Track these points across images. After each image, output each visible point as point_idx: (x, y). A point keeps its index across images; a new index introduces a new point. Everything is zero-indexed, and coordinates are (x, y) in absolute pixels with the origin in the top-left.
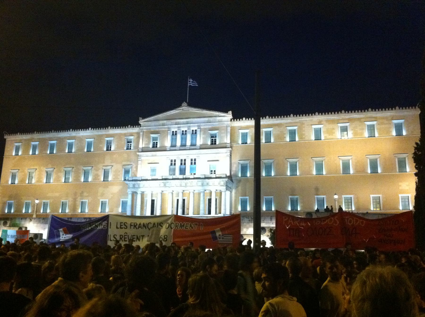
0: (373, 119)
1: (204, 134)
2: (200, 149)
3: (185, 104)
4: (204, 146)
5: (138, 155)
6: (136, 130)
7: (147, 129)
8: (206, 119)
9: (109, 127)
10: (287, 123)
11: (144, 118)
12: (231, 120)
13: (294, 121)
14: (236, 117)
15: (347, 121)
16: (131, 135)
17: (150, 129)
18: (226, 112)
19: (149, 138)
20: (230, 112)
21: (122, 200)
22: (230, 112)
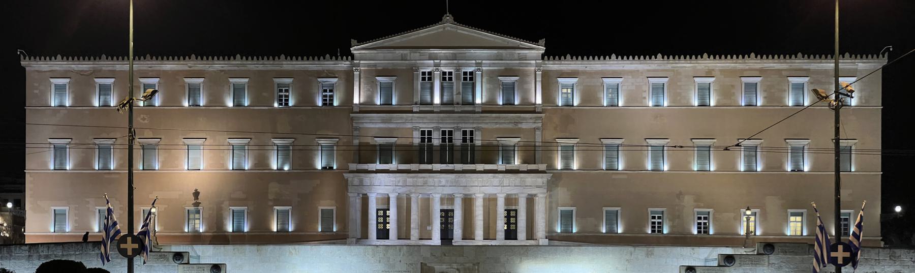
0: (804, 73)
1: (489, 82)
2: (483, 112)
3: (448, 17)
4: (488, 108)
5: (352, 119)
6: (344, 65)
7: (369, 65)
8: (495, 52)
9: (283, 56)
10: (648, 71)
11: (360, 41)
12: (543, 58)
13: (663, 67)
14: (552, 53)
15: (757, 73)
16: (331, 74)
17: (375, 65)
18: (535, 40)
19: (372, 84)
20: (543, 41)
21: (320, 208)
22: (543, 41)
